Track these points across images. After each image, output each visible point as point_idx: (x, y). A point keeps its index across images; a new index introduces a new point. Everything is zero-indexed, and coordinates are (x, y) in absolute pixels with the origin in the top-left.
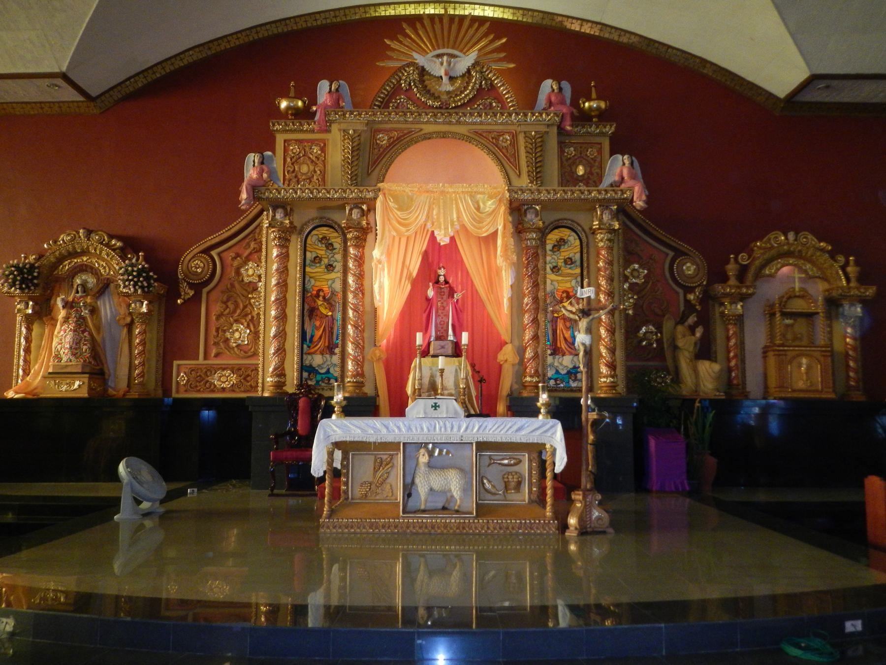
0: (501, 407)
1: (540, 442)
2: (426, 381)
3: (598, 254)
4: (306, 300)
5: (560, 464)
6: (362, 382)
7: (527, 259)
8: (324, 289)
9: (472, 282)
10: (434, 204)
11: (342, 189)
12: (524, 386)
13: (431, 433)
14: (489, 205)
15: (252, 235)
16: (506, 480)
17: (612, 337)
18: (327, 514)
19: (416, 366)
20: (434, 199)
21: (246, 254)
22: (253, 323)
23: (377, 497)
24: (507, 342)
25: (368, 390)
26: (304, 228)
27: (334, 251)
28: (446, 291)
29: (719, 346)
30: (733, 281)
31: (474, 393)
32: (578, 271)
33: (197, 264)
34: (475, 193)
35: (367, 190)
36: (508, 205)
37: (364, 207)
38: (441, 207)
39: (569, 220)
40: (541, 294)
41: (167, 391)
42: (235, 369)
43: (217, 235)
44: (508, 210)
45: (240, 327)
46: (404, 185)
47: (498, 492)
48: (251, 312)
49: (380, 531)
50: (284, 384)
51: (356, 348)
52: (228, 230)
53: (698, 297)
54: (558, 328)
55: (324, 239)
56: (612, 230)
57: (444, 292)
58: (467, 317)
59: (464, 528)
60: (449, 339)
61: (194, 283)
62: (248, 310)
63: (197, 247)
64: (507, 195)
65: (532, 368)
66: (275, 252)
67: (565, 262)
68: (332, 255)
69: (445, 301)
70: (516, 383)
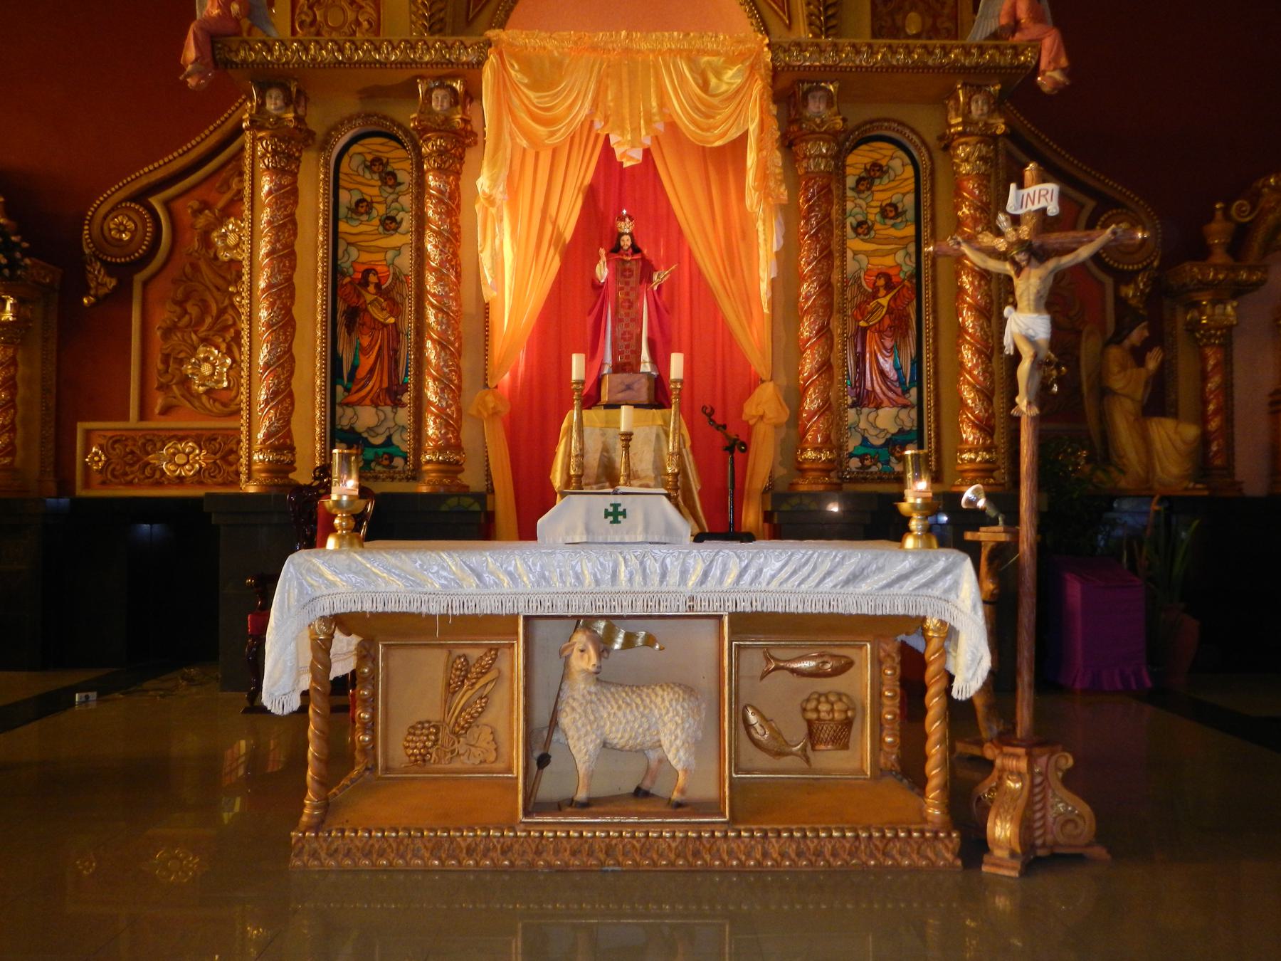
0: (751, 517)
1: (912, 613)
2: (593, 459)
3: (958, 191)
4: (339, 292)
5: (970, 675)
6: (457, 463)
7: (808, 201)
8: (378, 269)
9: (690, 252)
10: (608, 76)
11: (407, 41)
12: (801, 470)
13: (603, 588)
14: (732, 77)
15: (234, 163)
16: (813, 716)
17: (987, 367)
18: (311, 816)
19: (570, 428)
20: (608, 66)
21: (221, 204)
23: (456, 765)
24: (764, 378)
25: (471, 479)
26: (331, 136)
27: (398, 189)
28: (636, 268)
29: (1185, 390)
30: (1220, 257)
31: (695, 486)
32: (910, 231)
33: (121, 223)
34: (698, 51)
35: (462, 43)
36: (769, 80)
37: (458, 86)
38: (625, 84)
39: (895, 121)
40: (836, 277)
41: (65, 485)
42: (203, 439)
43: (161, 162)
44: (770, 91)
45: (212, 353)
46: (543, 34)
47: (787, 749)
48: (234, 324)
49: (460, 863)
50: (291, 466)
51: (443, 390)
52: (184, 152)
53: (1142, 291)
54: (868, 349)
55: (377, 165)
56: (989, 136)
57: (630, 270)
58: (681, 322)
59: (696, 854)
60: (642, 369)
61: (116, 263)
62: (228, 318)
63: (120, 187)
64: (768, 56)
65: (818, 431)
66: (266, 185)
67: (884, 213)
68: (392, 197)
69: (632, 289)
70: (781, 464)
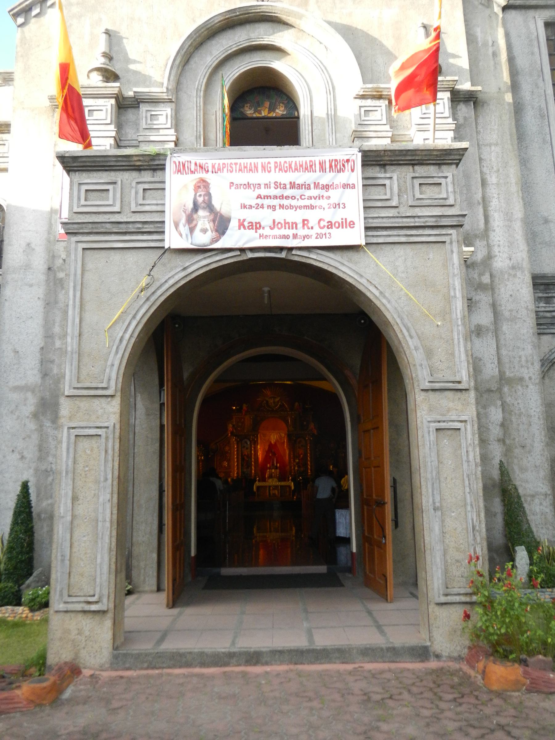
22: (229, 461)
